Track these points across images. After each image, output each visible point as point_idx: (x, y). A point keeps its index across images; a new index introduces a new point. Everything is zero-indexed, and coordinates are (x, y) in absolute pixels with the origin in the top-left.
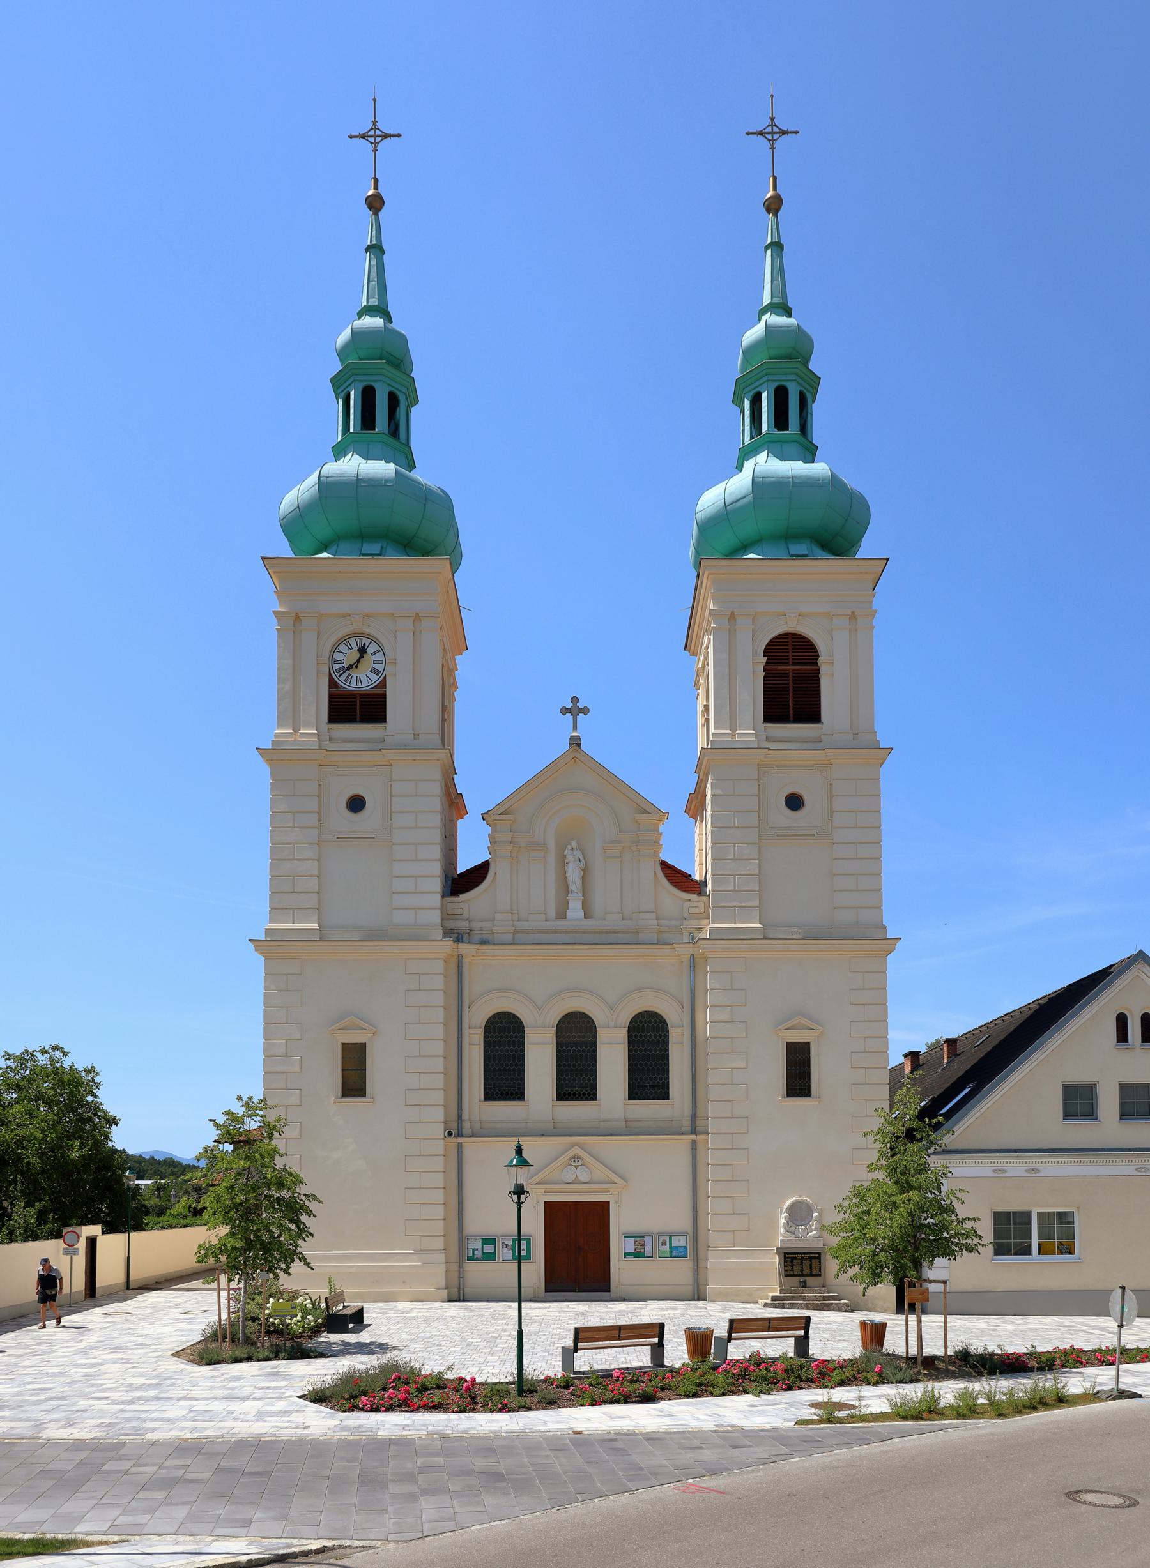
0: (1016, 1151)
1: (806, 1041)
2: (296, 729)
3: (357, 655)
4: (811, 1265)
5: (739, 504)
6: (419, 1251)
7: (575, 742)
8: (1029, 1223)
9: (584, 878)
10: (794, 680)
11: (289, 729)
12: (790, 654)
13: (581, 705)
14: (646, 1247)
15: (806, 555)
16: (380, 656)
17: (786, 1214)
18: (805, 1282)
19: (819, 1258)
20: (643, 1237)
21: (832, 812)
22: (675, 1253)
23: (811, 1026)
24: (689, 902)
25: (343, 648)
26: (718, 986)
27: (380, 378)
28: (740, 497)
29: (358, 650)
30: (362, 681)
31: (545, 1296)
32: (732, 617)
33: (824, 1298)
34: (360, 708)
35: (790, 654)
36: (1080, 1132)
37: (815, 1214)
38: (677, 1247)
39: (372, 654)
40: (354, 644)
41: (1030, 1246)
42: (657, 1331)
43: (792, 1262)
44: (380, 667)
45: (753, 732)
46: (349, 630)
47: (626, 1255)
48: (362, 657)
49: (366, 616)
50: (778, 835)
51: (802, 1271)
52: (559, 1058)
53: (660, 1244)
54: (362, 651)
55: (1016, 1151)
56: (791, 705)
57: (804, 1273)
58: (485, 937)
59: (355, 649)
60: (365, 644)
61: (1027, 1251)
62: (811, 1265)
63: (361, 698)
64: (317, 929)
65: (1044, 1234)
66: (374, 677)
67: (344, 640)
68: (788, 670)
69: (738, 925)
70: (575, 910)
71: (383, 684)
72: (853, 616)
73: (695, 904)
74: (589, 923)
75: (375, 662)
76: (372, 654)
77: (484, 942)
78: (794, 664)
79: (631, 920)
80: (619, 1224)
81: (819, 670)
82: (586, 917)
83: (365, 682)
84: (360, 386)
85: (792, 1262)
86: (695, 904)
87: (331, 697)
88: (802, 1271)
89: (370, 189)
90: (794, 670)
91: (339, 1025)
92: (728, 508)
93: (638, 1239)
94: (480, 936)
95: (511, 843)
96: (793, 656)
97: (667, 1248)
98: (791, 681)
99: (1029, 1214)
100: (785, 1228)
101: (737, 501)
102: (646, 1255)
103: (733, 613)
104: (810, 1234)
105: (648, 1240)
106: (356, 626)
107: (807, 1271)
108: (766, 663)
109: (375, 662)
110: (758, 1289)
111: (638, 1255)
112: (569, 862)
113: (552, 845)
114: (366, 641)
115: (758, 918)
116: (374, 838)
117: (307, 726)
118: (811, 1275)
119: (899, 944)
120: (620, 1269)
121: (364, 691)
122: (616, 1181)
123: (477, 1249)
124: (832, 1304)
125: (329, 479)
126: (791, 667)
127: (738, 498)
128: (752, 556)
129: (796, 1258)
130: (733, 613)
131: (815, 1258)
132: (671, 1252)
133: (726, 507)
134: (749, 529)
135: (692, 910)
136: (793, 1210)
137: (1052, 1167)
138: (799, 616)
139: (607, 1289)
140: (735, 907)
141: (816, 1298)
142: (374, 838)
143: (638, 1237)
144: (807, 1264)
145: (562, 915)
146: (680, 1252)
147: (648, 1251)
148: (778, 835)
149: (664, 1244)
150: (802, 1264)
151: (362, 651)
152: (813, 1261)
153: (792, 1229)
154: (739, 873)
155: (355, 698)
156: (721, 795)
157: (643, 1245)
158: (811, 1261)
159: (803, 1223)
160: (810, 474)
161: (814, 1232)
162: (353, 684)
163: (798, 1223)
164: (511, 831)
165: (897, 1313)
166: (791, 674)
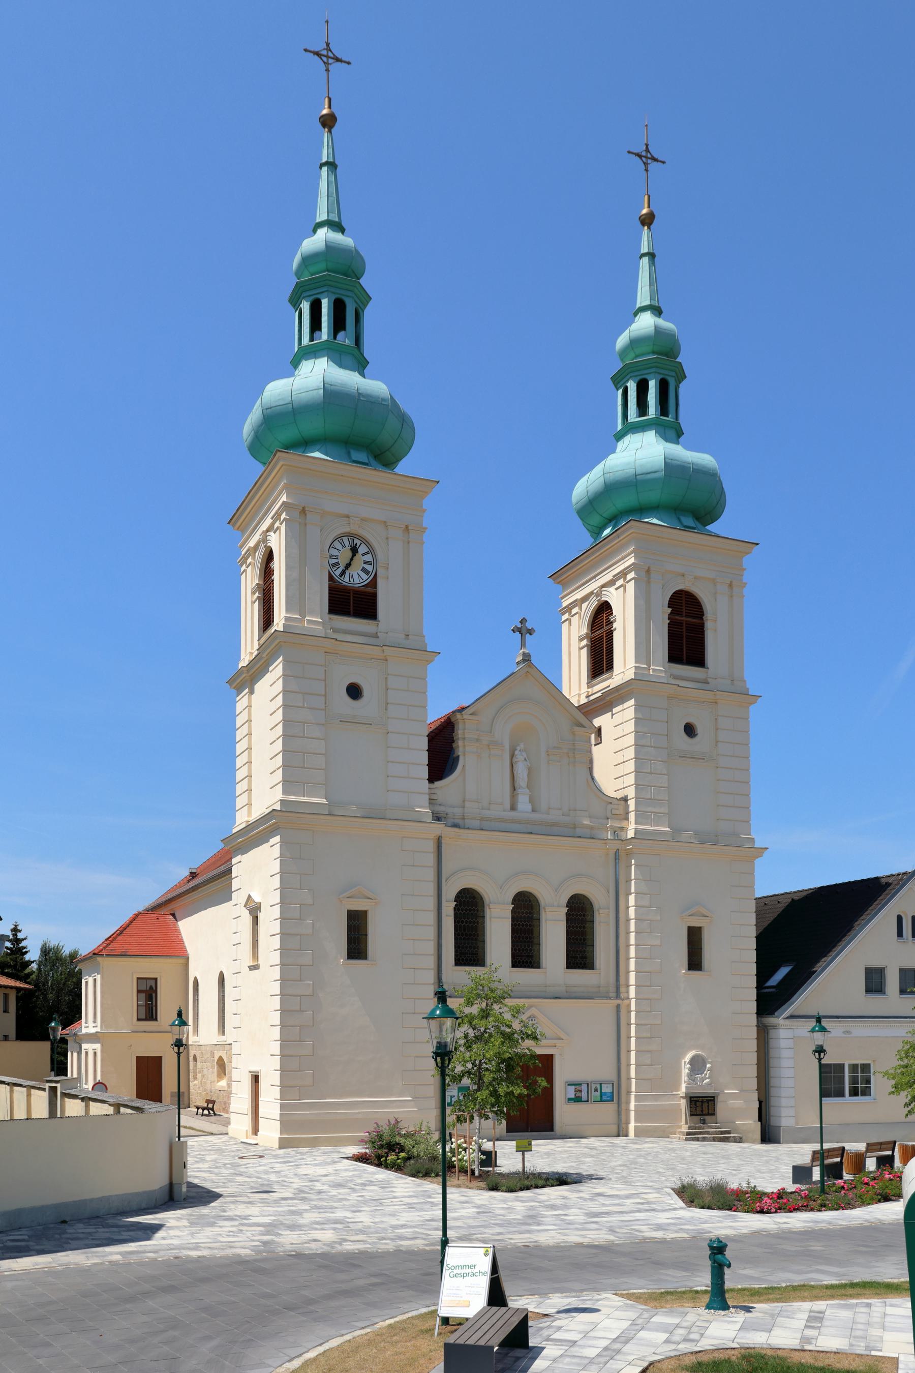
0: (837, 1017)
1: (699, 926)
2: (303, 616)
3: (350, 554)
4: (708, 1106)
5: (649, 476)
6: (415, 1098)
7: (527, 658)
8: (843, 1072)
9: (529, 775)
10: (686, 630)
11: (296, 614)
12: (684, 607)
13: (529, 625)
14: (583, 1093)
15: (694, 528)
16: (368, 558)
17: (688, 1066)
18: (704, 1120)
19: (714, 1100)
20: (581, 1084)
21: (717, 742)
22: (604, 1098)
23: (705, 914)
24: (610, 805)
25: (337, 544)
26: (641, 878)
27: (350, 294)
28: (651, 471)
29: (351, 549)
30: (356, 578)
31: (507, 1136)
32: (648, 571)
33: (722, 1133)
34: (354, 603)
35: (684, 607)
36: (875, 1004)
37: (708, 1066)
38: (605, 1093)
39: (363, 555)
40: (347, 543)
41: (843, 1089)
42: (840, 1152)
43: (695, 1104)
44: (369, 568)
45: (645, 666)
46: (346, 529)
47: (569, 1099)
48: (354, 555)
49: (363, 520)
50: (680, 756)
51: (702, 1111)
52: (514, 931)
53: (593, 1090)
54: (354, 550)
55: (837, 1017)
56: (685, 650)
57: (704, 1113)
58: (456, 821)
59: (348, 548)
60: (356, 544)
61: (841, 1094)
62: (708, 1106)
63: (354, 594)
64: (326, 804)
65: (854, 1081)
66: (365, 576)
67: (339, 538)
68: (683, 620)
69: (654, 828)
70: (524, 803)
71: (373, 583)
72: (731, 585)
73: (616, 807)
74: (513, 814)
75: (365, 562)
76: (363, 555)
77: (455, 826)
78: (686, 616)
79: (568, 815)
80: (562, 1074)
81: (704, 624)
82: (533, 811)
83: (357, 581)
84: (333, 297)
85: (695, 1104)
86: (616, 807)
87: (331, 589)
88: (702, 1111)
89: (644, 208)
90: (686, 621)
91: (347, 894)
92: (638, 477)
93: (577, 1087)
94: (453, 820)
95: (477, 741)
96: (686, 609)
97: (598, 1093)
98: (684, 630)
99: (842, 1066)
100: (688, 1077)
101: (647, 473)
102: (583, 1100)
103: (649, 568)
104: (705, 1081)
105: (584, 1087)
106: (354, 528)
107: (705, 1112)
108: (671, 613)
109: (365, 562)
110: (669, 1127)
111: (577, 1099)
112: (518, 761)
113: (507, 747)
114: (356, 541)
115: (667, 823)
116: (371, 724)
117: (312, 613)
118: (709, 1114)
119: (766, 852)
120: (563, 1112)
121: (357, 587)
122: (562, 1036)
123: (454, 1096)
124: (730, 1137)
125: (673, 461)
126: (684, 619)
127: (649, 472)
128: (655, 521)
129: (698, 1101)
130: (649, 568)
131: (711, 1100)
132: (601, 1096)
133: (636, 476)
134: (653, 496)
135: (614, 812)
136: (693, 1061)
137: (860, 1030)
138: (695, 578)
139: (551, 1129)
140: (652, 813)
141: (716, 1133)
142: (371, 724)
143: (577, 1085)
144: (705, 1105)
145: (513, 808)
146: (608, 1097)
147: (584, 1096)
148: (680, 756)
149: (596, 1090)
150: (702, 1106)
151: (354, 550)
152: (710, 1103)
153: (693, 1077)
154: (653, 785)
155: (349, 593)
156: (641, 719)
157: (581, 1091)
158: (708, 1103)
159: (699, 1072)
160: (703, 463)
161: (708, 1080)
162: (347, 579)
163: (696, 1072)
164: (477, 730)
165: (762, 1143)
166: (684, 624)
